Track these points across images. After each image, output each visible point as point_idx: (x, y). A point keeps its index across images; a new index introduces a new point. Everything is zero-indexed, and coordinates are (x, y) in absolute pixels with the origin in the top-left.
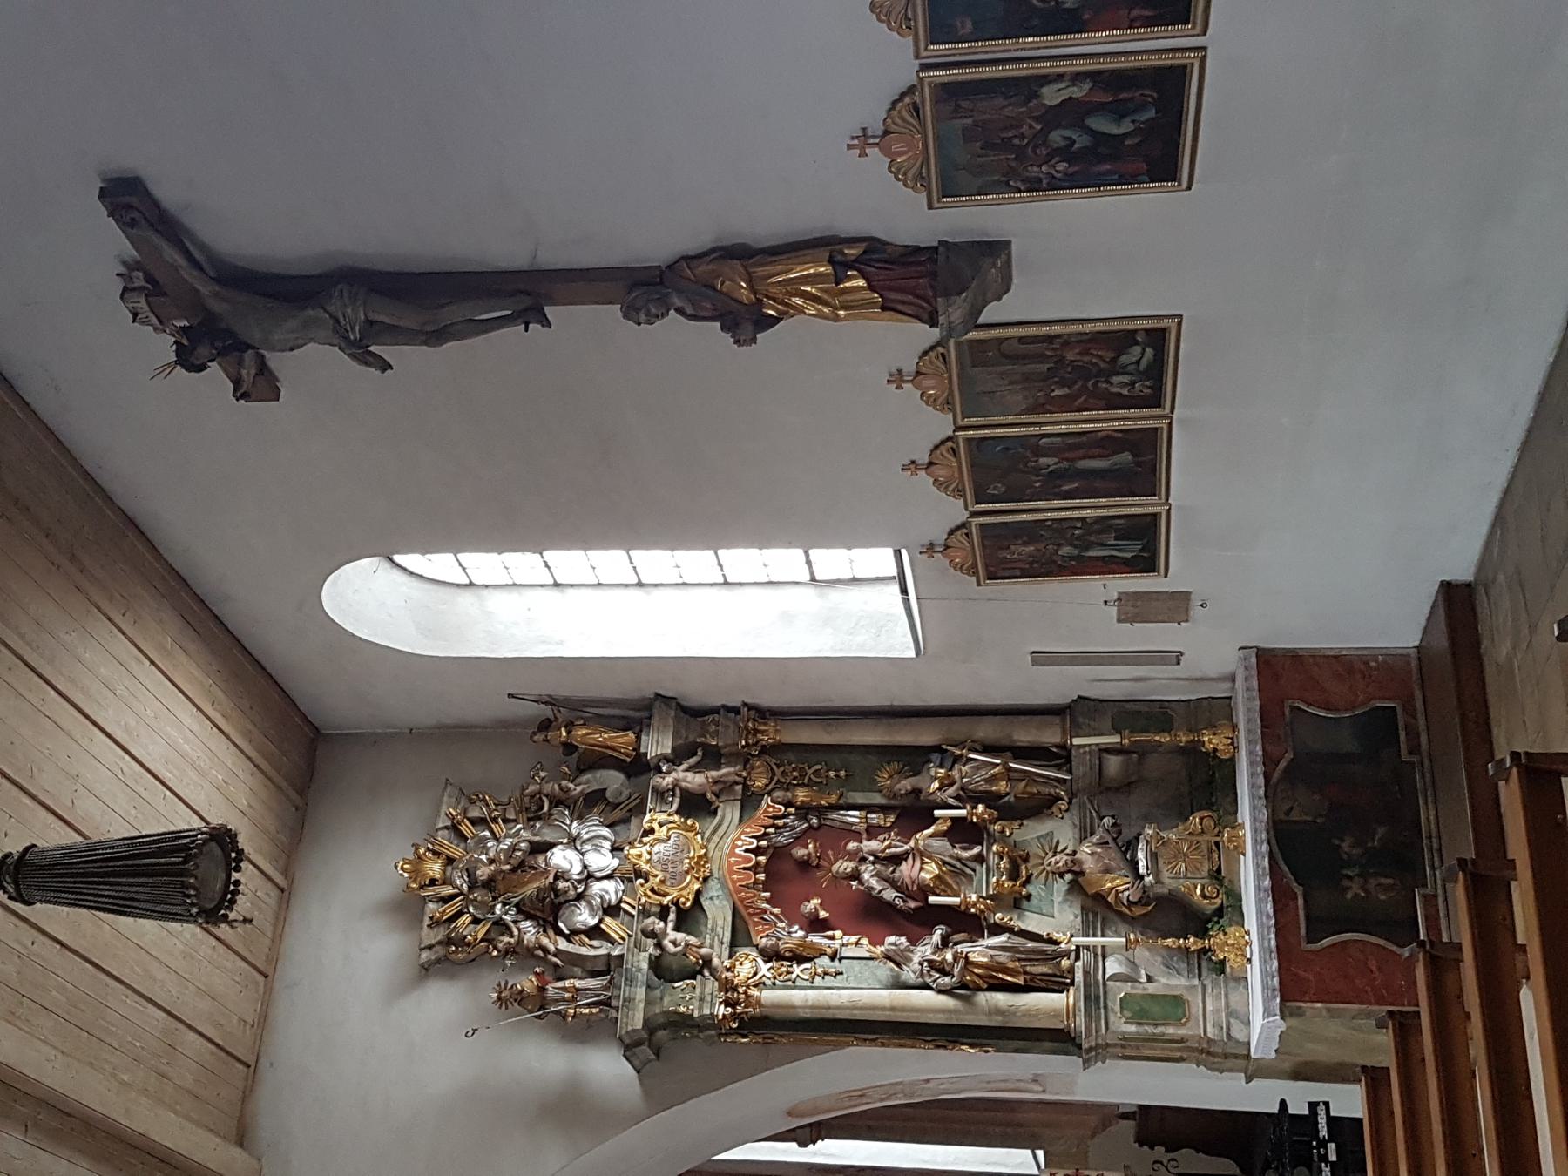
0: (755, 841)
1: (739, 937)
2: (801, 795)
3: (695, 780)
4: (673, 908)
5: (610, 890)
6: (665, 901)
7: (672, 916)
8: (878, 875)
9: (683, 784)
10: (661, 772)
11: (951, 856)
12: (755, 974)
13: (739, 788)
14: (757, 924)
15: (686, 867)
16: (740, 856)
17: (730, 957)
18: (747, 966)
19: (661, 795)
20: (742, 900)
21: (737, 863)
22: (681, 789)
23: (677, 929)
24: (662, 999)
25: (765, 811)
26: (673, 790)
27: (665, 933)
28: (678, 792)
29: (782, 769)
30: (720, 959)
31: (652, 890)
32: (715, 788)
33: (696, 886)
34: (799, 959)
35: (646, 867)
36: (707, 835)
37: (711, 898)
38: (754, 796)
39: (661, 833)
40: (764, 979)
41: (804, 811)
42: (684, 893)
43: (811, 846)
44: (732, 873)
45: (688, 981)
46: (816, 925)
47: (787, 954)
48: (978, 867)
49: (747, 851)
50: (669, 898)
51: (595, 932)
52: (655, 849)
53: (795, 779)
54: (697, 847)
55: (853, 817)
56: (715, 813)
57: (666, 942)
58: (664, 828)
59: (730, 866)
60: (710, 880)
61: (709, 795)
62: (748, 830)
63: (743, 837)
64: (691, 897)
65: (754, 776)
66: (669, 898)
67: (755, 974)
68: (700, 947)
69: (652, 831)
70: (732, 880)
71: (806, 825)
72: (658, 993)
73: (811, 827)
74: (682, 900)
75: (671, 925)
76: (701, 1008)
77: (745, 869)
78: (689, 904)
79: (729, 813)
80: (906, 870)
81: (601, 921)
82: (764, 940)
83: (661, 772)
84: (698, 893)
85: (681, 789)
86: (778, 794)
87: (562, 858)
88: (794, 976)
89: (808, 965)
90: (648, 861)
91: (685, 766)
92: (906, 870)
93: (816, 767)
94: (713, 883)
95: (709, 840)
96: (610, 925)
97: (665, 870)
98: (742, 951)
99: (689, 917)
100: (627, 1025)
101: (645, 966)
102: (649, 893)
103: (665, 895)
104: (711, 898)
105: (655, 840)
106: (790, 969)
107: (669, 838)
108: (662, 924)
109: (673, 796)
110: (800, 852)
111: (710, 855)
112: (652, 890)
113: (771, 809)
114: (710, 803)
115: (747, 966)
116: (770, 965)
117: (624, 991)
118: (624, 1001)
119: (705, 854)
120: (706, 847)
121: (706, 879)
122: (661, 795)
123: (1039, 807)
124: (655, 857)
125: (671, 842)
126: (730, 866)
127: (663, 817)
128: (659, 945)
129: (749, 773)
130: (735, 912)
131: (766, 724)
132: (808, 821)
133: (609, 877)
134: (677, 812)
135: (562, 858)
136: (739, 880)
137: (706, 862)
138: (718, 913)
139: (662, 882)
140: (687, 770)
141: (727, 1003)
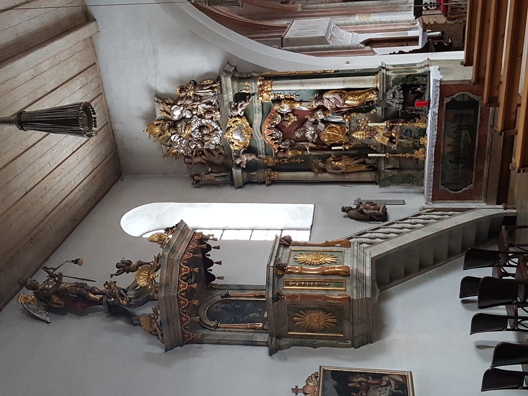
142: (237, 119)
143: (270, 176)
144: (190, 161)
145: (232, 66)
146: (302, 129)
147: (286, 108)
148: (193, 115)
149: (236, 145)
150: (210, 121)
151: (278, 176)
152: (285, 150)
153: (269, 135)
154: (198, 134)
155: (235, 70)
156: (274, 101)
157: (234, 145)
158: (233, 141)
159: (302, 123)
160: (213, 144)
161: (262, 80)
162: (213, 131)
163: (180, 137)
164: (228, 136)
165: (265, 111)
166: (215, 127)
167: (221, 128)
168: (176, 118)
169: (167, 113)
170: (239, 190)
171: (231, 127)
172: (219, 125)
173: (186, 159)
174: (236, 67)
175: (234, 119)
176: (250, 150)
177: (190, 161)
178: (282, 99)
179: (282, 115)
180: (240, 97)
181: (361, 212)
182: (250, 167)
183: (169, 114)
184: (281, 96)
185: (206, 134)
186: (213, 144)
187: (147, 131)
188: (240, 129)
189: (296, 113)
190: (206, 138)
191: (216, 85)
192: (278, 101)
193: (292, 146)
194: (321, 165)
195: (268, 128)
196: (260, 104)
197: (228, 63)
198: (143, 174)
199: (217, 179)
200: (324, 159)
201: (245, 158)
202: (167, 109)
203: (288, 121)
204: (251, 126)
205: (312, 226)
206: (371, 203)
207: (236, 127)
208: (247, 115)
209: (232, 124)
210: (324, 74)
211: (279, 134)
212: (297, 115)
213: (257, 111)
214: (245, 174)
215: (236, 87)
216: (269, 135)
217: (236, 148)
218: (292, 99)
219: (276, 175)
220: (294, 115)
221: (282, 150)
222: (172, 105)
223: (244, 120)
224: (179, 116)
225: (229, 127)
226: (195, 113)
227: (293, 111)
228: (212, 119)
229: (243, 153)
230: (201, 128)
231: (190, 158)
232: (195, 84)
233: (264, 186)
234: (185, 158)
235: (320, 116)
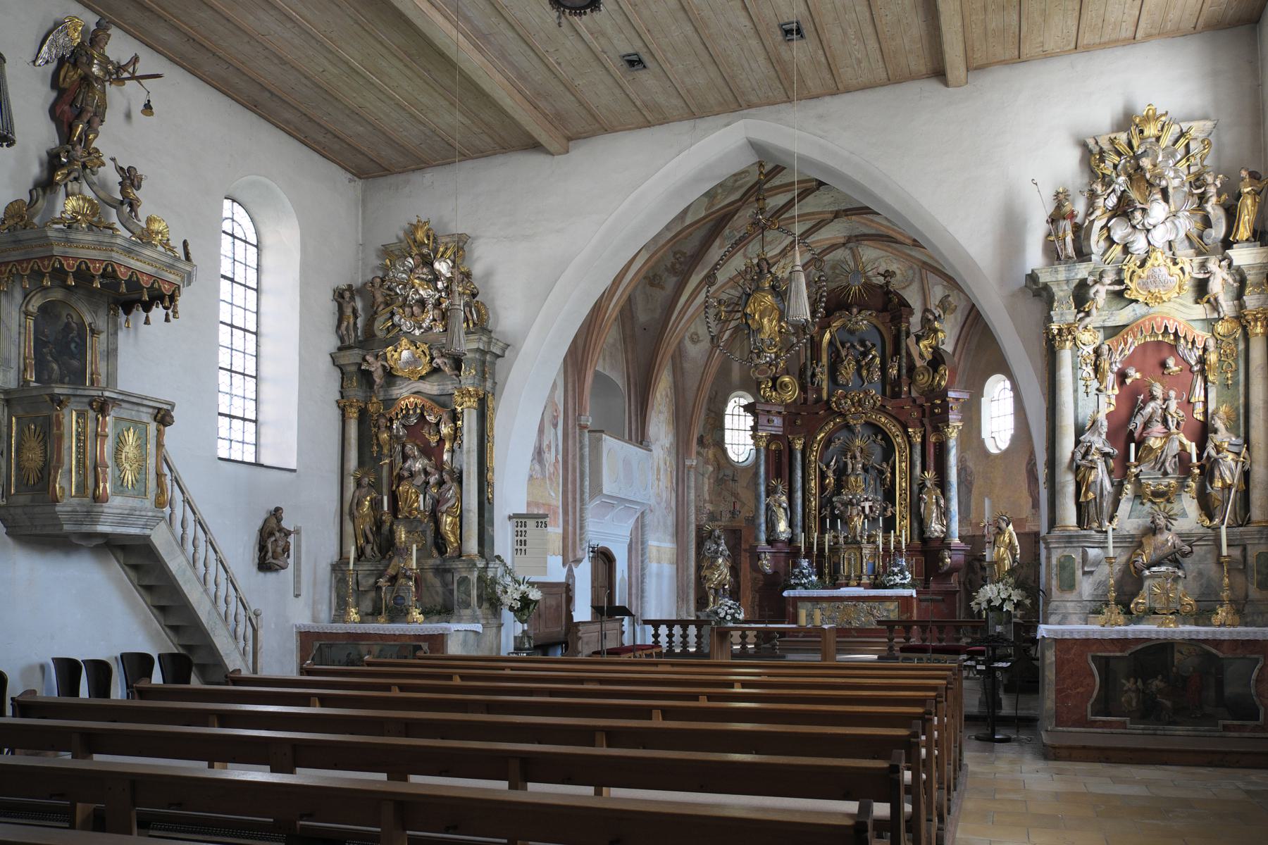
0: (1174, 331)
1: (1113, 332)
2: (1212, 358)
3: (1216, 287)
4: (1123, 287)
5: (1139, 245)
6: (1127, 281)
7: (1117, 288)
8: (1154, 412)
9: (1212, 279)
10: (1220, 261)
11: (1167, 455)
12: (1084, 344)
13: (1216, 316)
14: (1117, 341)
15: (1153, 291)
16: (1162, 323)
17: (1094, 328)
18: (1089, 339)
19: (1203, 266)
20: (1132, 330)
21: (1156, 323)
22: (1208, 278)
23: (1108, 292)
24: (1062, 290)
25: (1198, 336)
26: (1208, 273)
27: (1104, 285)
28: (1207, 276)
29: (1231, 342)
30: (1095, 320)
31: (1134, 272)
32: (1212, 299)
33: (1141, 299)
34: (1097, 368)
35: (1148, 265)
36: (1178, 300)
37: (1134, 310)
38: (1211, 327)
39: (1176, 270)
40: (1081, 350)
41: (1202, 361)
42: (1135, 293)
43: (1177, 369)
44: (1150, 320)
45: (1073, 305)
46: (1122, 376)
47: (1098, 362)
48: (1160, 472)
49: (1166, 327)
50: (1129, 284)
51: (1111, 242)
52: (1162, 268)
53: (1225, 351)
54: (1169, 295)
55: (1199, 394)
56: (1197, 303)
57: (1098, 287)
58: (1180, 272)
59: (1155, 318)
60: (1147, 307)
61: (1207, 297)
62: (1182, 327)
63: (1176, 323)
64: (1133, 297)
65: (1226, 324)
66: (1129, 284)
67: (1084, 344)
68: (1096, 308)
69: (1175, 263)
70: (1144, 322)
71: (1193, 363)
72: (1065, 288)
73: (1191, 366)
74: (1129, 292)
75: (1111, 288)
76: (1057, 314)
77: (1153, 328)
78: (1126, 296)
79: (1200, 311)
80: (1158, 428)
81: (1118, 244)
82: (1107, 347)
83: (1220, 261)
84: (1137, 301)
85: (1208, 278)
86: (1211, 343)
87: (1158, 210)
88: (1084, 367)
89: (1092, 375)
90: (1153, 265)
91: (1226, 277)
92: (1158, 428)
93: (1233, 364)
94: (1145, 309)
95: (1175, 302)
96: (1117, 250)
97: (1148, 277)
98: (1101, 335)
99: (1119, 296)
100: (1041, 273)
101: (1080, 276)
102: (1131, 270)
103: (1131, 280)
104: (1134, 310)
105: (1169, 267)
106: (1089, 365)
107: (1172, 276)
108: (1110, 282)
109: (1205, 273)
110: (1171, 362)
111: (1165, 304)
112: (1134, 272)
113: (1200, 339)
114: (1202, 299)
115: (1089, 339)
116: (1091, 353)
117: (1062, 268)
118: (1056, 268)
119: (1164, 301)
120: (1169, 301)
121: (1147, 304)
122: (1203, 266)
123: (1207, 506)
124: (1156, 269)
125: (1169, 278)
126: (1155, 318)
127: (1187, 269)
128: (1095, 282)
129: (1227, 321)
130: (1124, 326)
131: (1262, 326)
132: (1196, 364)
133: (1149, 243)
134: (1191, 277)
135: (1158, 210)
136: (1145, 326)
137: (1159, 303)
138: (1123, 316)
139: (1140, 277)
140: (1224, 279)
141: (1060, 330)
142: (428, 358)
143: (351, 406)
144: (377, 285)
145: (504, 352)
146: (416, 453)
147: (445, 430)
148: (440, 291)
149: (393, 355)
150: (431, 317)
151: (351, 418)
152: (390, 428)
153: (407, 405)
154: (413, 299)
155: (498, 356)
156: (454, 411)
157: (393, 352)
158: (399, 350)
159: (427, 451)
160: (400, 320)
161: (477, 394)
162: (417, 322)
163: (411, 271)
164: (403, 344)
165: (443, 398)
166: (424, 325)
167: (422, 333)
168: (437, 265)
169: (444, 253)
170: (329, 358)
171: (417, 348)
172: (426, 331)
173: (378, 280)
174: (503, 356)
175: (427, 352)
176: (390, 376)
177: (377, 285)
178: (456, 424)
179: (438, 424)
180: (457, 363)
181: (271, 534)
182: (366, 376)
183: (442, 256)
184: (460, 423)
185: (413, 312)
186: (400, 320)
187: (419, 221)
188: (414, 361)
189: (441, 443)
190: (407, 309)
191: (471, 326)
192: (455, 417)
193: (395, 438)
194: (365, 481)
195: (416, 404)
196: (450, 392)
197: (509, 346)
198: (363, 212)
199: (345, 323)
200: (377, 486)
201: (375, 367)
202: (449, 253)
203: (430, 433)
204: (422, 378)
205: (262, 465)
206: (286, 549)
207: (417, 356)
208: (436, 370)
209: (420, 349)
210: (486, 483)
211: (413, 420)
212: (438, 445)
213: (441, 387)
214: (353, 368)
215: (469, 355)
216: (407, 405)
217: (389, 355)
218: (455, 439)
219: (353, 414)
220: (437, 442)
221: (388, 424)
222: (454, 262)
223: (428, 369)
224: (440, 272)
225: (416, 345)
226: (443, 294)
227: (441, 441)
228: (434, 320)
229: (383, 366)
230: (422, 303)
231: (381, 286)
232: (474, 295)
233: (338, 397)
234: (381, 278)
235: (432, 480)
